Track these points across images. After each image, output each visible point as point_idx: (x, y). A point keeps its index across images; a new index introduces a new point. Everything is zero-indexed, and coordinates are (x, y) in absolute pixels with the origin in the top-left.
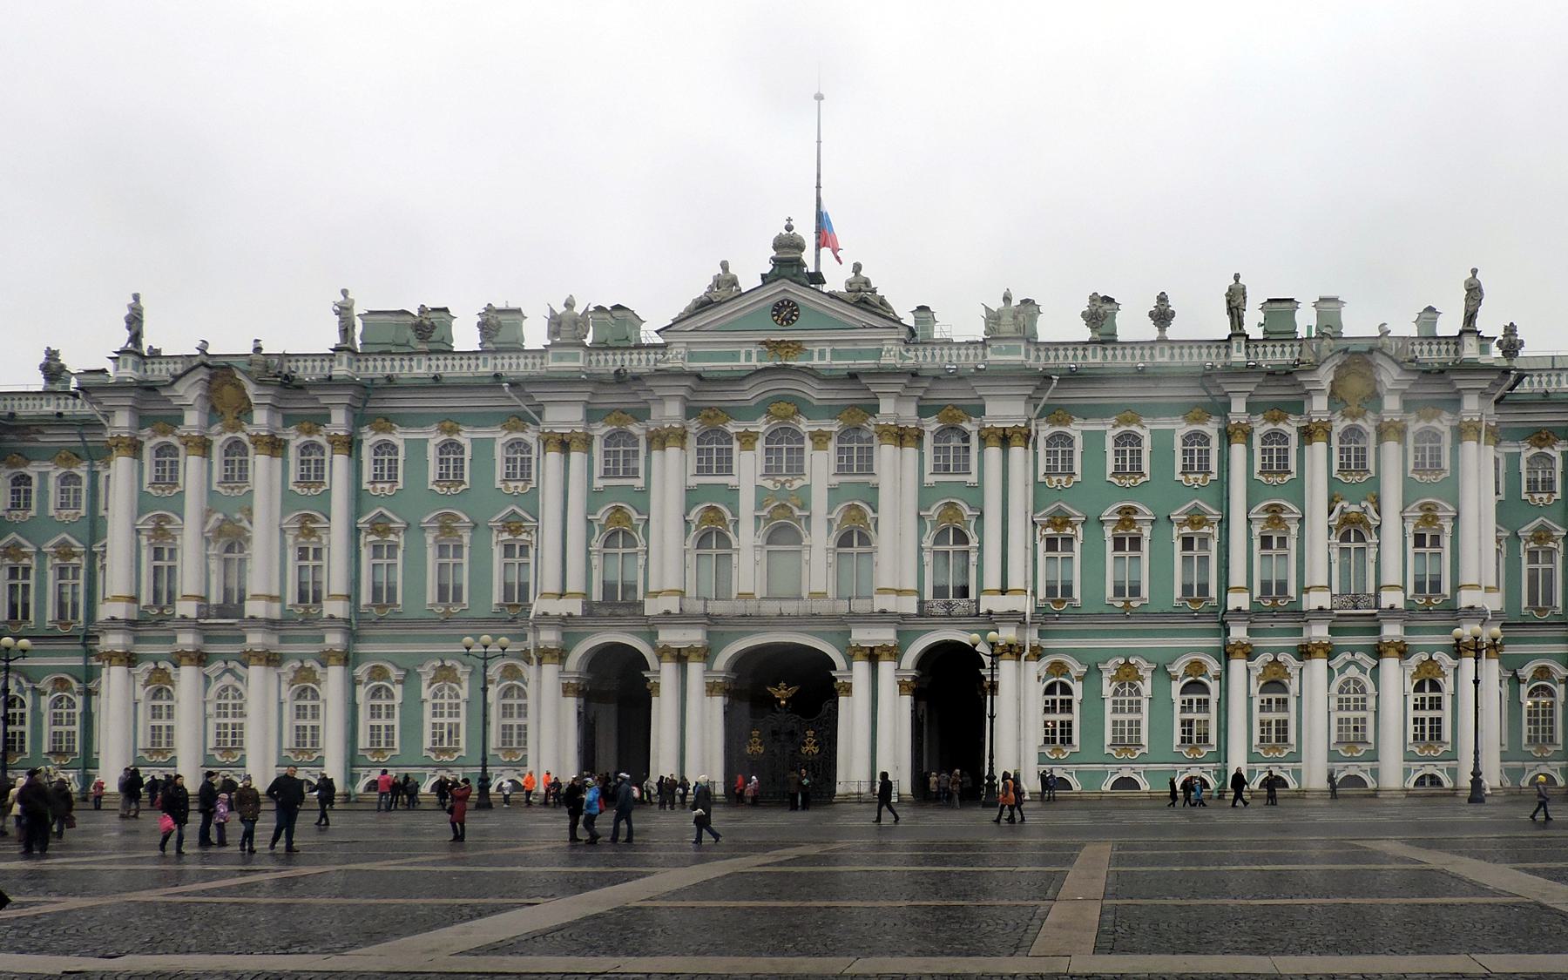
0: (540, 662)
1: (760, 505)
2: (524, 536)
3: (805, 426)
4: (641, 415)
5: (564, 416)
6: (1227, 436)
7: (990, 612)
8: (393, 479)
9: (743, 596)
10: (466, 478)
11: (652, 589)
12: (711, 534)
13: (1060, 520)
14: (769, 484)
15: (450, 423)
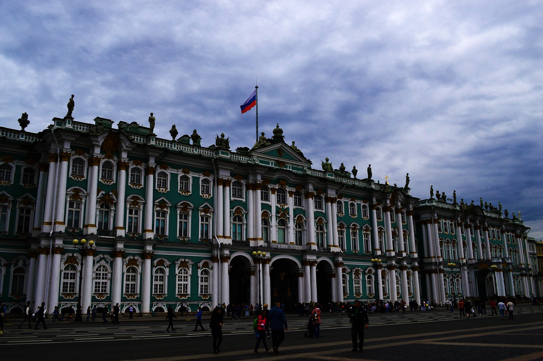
0: (222, 262)
1: (278, 212)
2: (208, 214)
3: (288, 189)
4: (246, 178)
5: (224, 174)
6: (372, 207)
7: (333, 252)
8: (165, 186)
9: (274, 242)
10: (191, 190)
11: (251, 236)
12: (266, 221)
13: (341, 226)
14: (279, 206)
15: (186, 170)
